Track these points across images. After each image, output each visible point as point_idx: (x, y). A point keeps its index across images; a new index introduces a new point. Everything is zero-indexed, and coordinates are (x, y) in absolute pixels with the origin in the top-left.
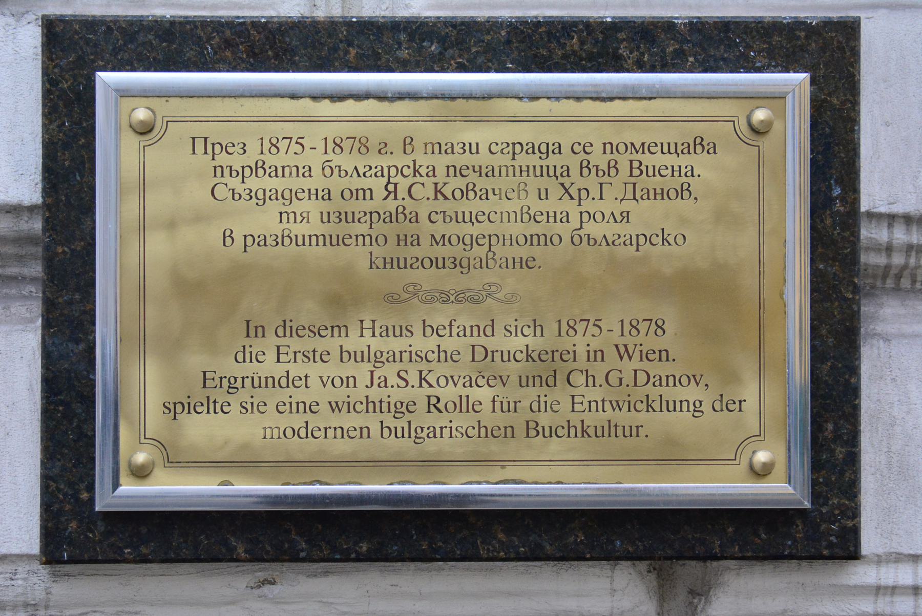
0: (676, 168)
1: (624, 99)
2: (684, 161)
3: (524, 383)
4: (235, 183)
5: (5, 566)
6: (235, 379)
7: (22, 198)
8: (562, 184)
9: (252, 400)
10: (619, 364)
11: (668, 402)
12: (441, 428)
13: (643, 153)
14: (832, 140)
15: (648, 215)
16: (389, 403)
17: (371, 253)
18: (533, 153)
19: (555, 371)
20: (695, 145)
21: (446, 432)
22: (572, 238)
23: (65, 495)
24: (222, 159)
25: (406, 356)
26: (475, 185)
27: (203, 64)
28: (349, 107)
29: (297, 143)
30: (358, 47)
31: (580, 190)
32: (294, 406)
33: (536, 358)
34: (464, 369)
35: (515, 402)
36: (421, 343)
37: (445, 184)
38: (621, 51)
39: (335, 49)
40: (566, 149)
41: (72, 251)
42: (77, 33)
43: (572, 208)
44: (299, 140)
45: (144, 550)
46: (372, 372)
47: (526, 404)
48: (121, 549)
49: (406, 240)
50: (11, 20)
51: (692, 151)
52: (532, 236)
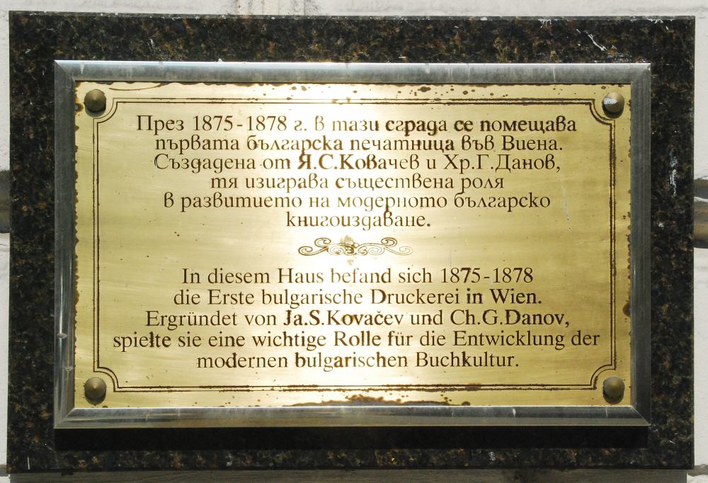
2: (550, 135)
4: (174, 154)
6: (175, 317)
8: (447, 156)
11: (534, 337)
13: (515, 130)
14: (670, 119)
16: (303, 338)
22: (455, 200)
24: (164, 134)
31: (462, 161)
32: (224, 340)
33: (425, 301)
37: (350, 155)
40: (450, 126)
42: (39, 26)
44: (228, 119)
46: (289, 312)
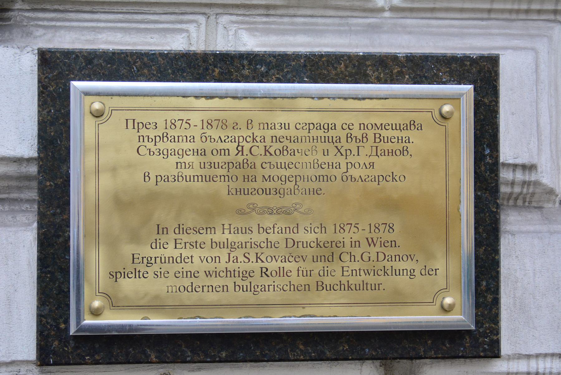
0: (400, 138)
1: (371, 99)
2: (404, 134)
3: (315, 260)
4: (151, 145)
5: (13, 367)
6: (151, 258)
7: (24, 153)
8: (336, 147)
9: (160, 270)
10: (368, 249)
11: (396, 270)
12: (269, 286)
13: (382, 129)
14: (484, 123)
15: (385, 164)
16: (239, 271)
17: (229, 186)
18: (320, 129)
19: (333, 253)
20: (410, 125)
21: (271, 288)
22: (342, 177)
23: (51, 325)
24: (144, 132)
25: (248, 245)
26: (287, 147)
27: (131, 77)
28: (216, 103)
29: (186, 123)
30: (220, 68)
31: (346, 150)
32: (185, 274)
33: (322, 246)
34: (282, 251)
35: (310, 271)
36: (257, 237)
37: (271, 146)
38: (368, 72)
39: (207, 69)
40: (338, 127)
41: (56, 184)
42: (58, 58)
43: (342, 160)
44: (188, 121)
45: (97, 357)
46: (229, 254)
47: (316, 272)
48: (84, 357)
49: (248, 178)
50: (18, 51)
51: (409, 128)
52: (319, 176)
